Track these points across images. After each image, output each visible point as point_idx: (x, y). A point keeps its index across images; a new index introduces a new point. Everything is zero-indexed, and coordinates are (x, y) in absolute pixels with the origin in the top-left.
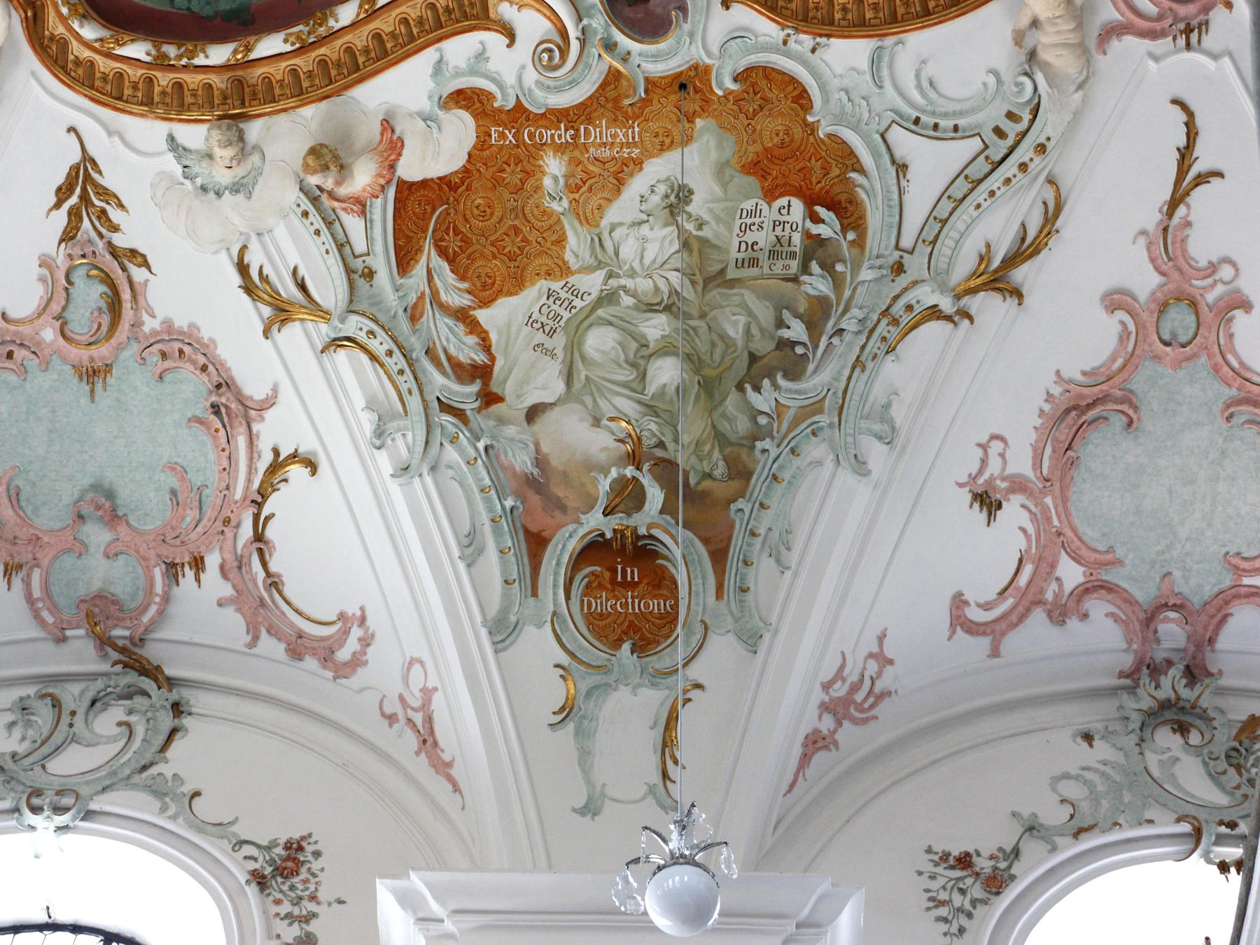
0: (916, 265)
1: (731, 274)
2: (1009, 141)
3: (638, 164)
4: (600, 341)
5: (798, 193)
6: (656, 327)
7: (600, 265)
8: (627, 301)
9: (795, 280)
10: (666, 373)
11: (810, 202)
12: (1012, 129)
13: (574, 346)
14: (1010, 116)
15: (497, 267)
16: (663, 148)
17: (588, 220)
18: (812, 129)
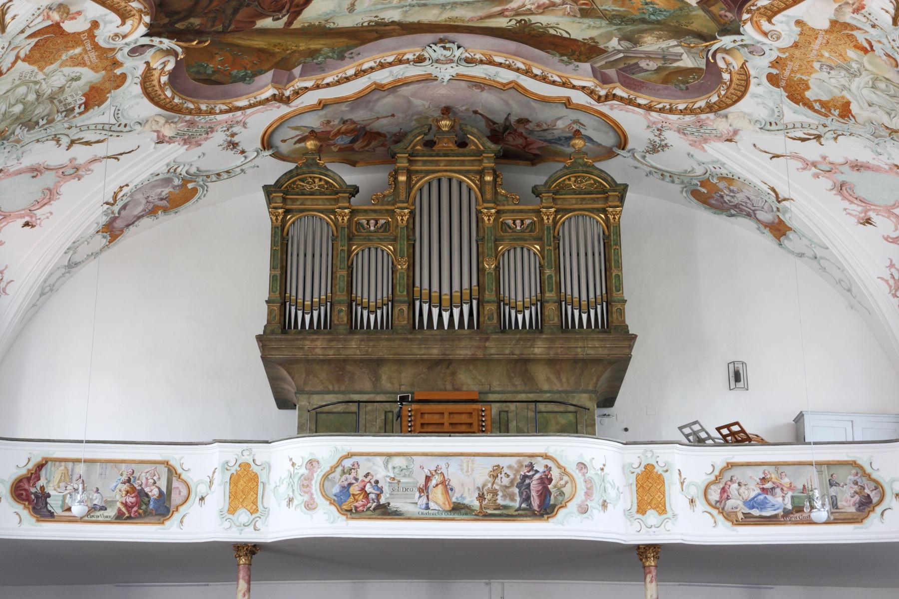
0: (74, 130)
1: (55, 101)
2: (117, 128)
3: (85, 65)
4: (22, 90)
5: (87, 99)
6: (32, 97)
7: (47, 75)
8: (37, 87)
9: (58, 112)
10: (18, 109)
11: (84, 103)
12: (122, 128)
13: (18, 86)
14: (125, 126)
15: (37, 55)
16: (92, 69)
17: (61, 66)
18: (109, 92)
